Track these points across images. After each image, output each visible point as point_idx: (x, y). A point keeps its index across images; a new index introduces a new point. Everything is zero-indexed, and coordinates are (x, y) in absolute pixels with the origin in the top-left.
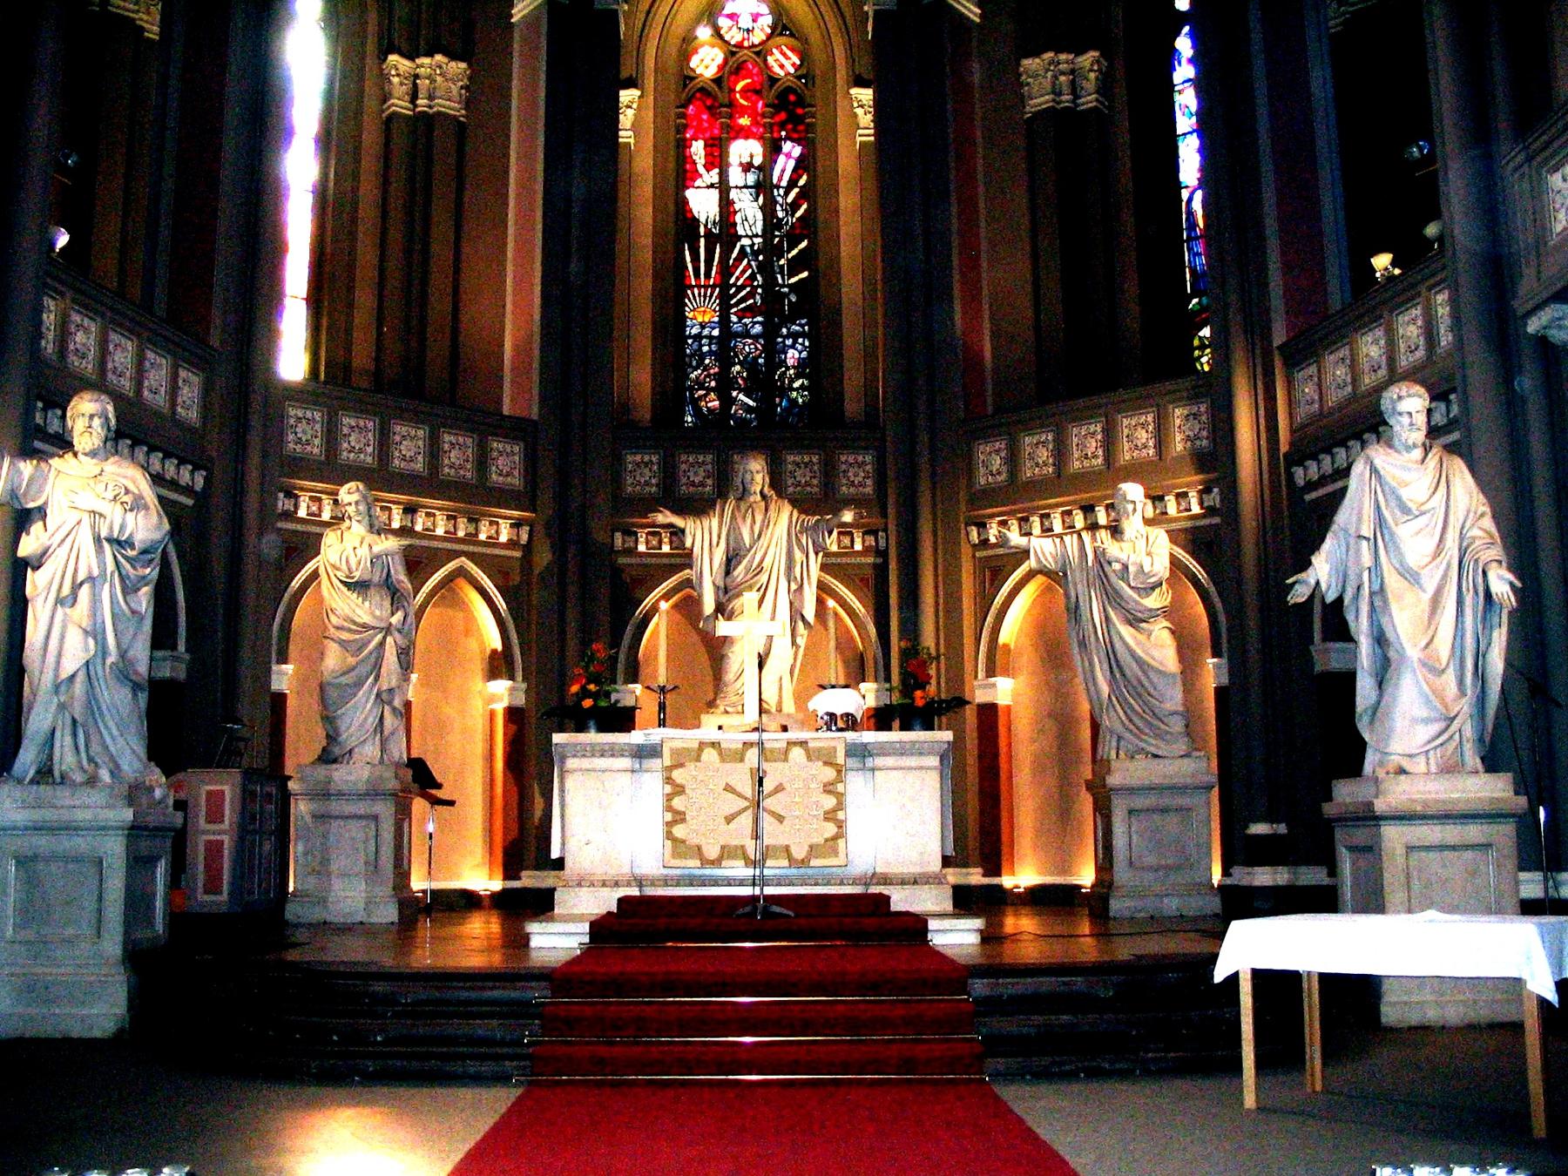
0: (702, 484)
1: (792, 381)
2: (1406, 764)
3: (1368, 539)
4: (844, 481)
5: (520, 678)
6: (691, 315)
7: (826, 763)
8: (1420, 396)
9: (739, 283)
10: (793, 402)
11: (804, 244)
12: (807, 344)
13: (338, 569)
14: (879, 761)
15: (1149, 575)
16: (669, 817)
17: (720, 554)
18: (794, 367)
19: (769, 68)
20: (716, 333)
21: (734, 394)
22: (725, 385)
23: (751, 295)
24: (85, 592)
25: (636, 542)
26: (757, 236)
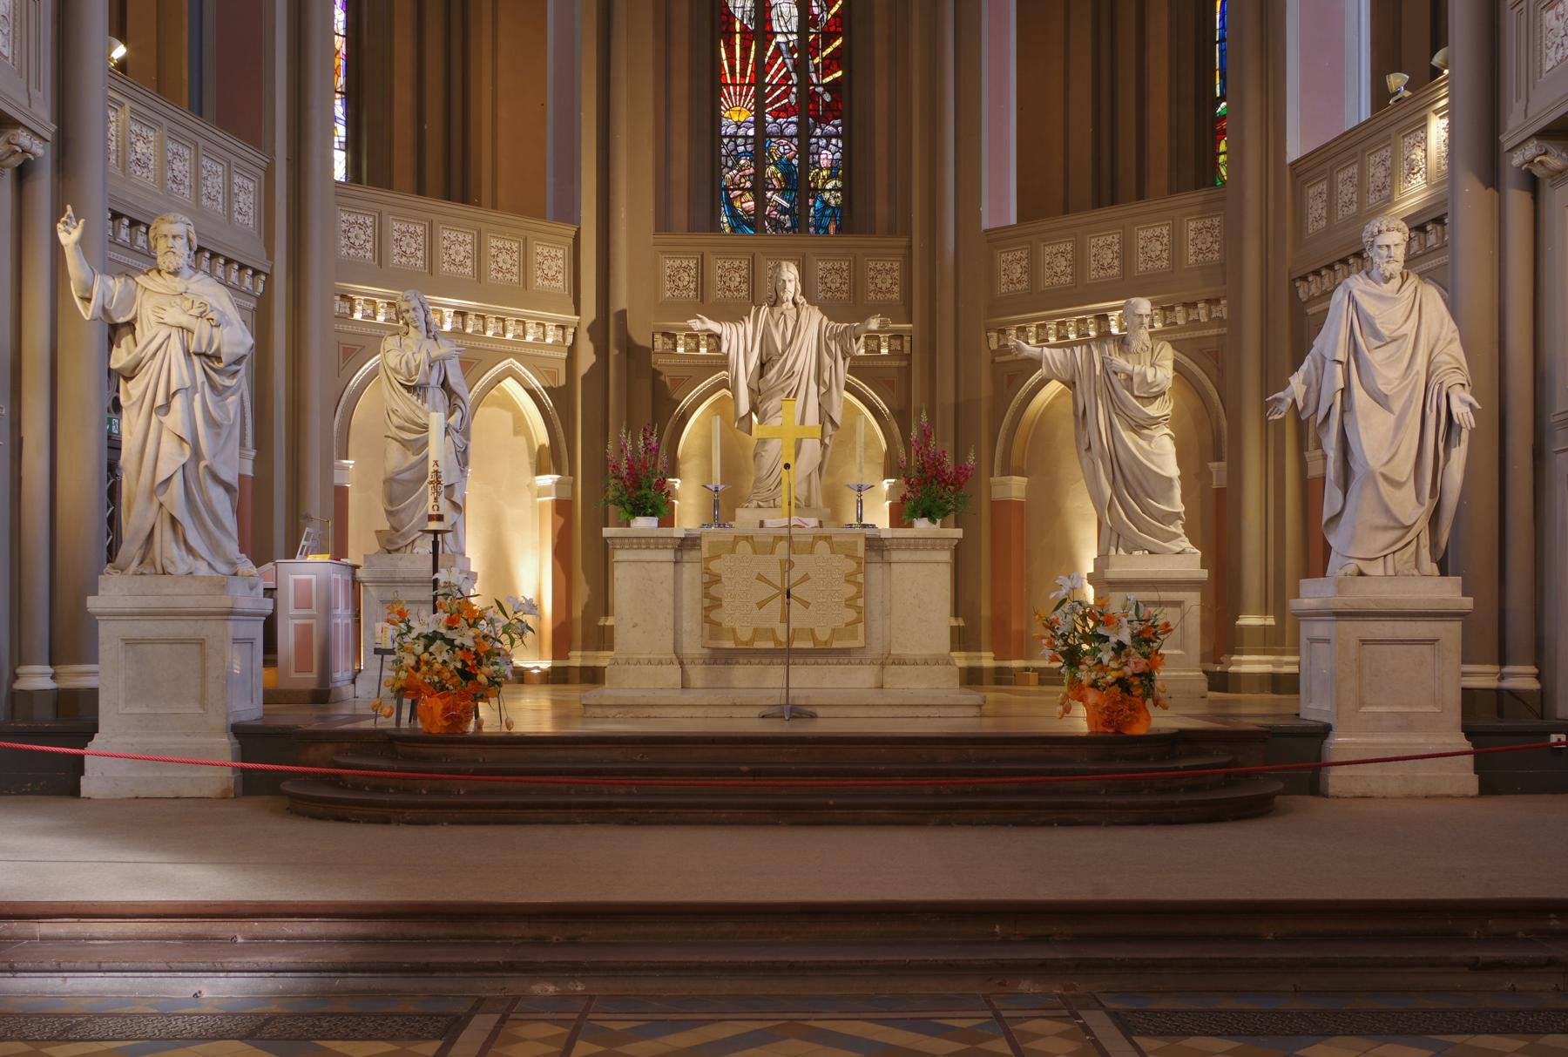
1: (825, 182)
2: (1364, 566)
3: (1341, 362)
4: (872, 287)
5: (567, 472)
6: (727, 115)
7: (847, 556)
8: (1398, 230)
9: (774, 82)
10: (826, 204)
11: (838, 42)
12: (840, 145)
13: (398, 373)
14: (895, 556)
15: (1151, 385)
16: (707, 602)
18: (827, 169)
20: (751, 132)
21: (769, 194)
22: (759, 187)
23: (786, 94)
24: (177, 402)
25: (675, 345)
26: (791, 33)
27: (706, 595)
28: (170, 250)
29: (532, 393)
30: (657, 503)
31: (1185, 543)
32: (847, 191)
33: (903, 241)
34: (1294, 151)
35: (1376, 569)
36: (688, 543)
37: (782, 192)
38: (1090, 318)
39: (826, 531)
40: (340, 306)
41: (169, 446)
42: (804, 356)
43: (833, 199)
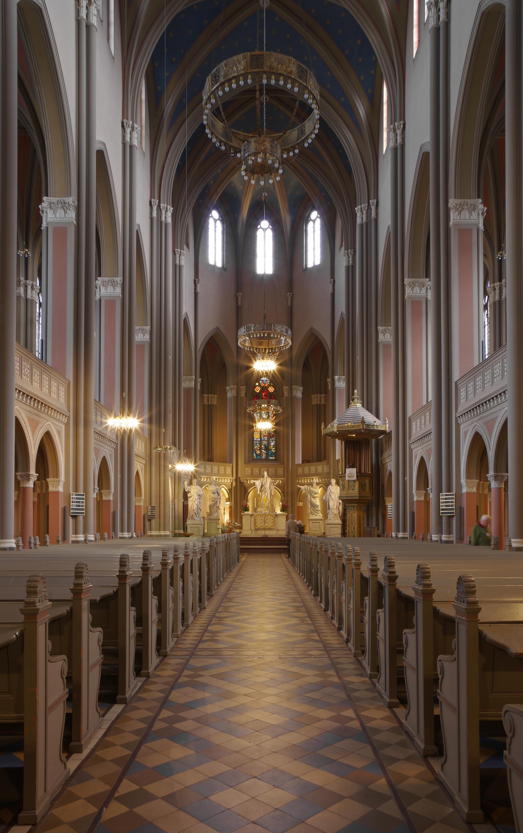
0: (257, 473)
10: (272, 452)
14: (279, 517)
17: (260, 486)
19: (269, 391)
20: (259, 440)
22: (260, 449)
24: (196, 501)
27: (254, 522)
28: (195, 483)
29: (226, 490)
30: (246, 509)
31: (321, 514)
32: (276, 450)
33: (284, 465)
34: (337, 458)
35: (332, 519)
36: (252, 515)
37: (265, 450)
38: (311, 479)
39: (270, 513)
40: (200, 479)
41: (195, 505)
42: (268, 485)
43: (274, 451)
